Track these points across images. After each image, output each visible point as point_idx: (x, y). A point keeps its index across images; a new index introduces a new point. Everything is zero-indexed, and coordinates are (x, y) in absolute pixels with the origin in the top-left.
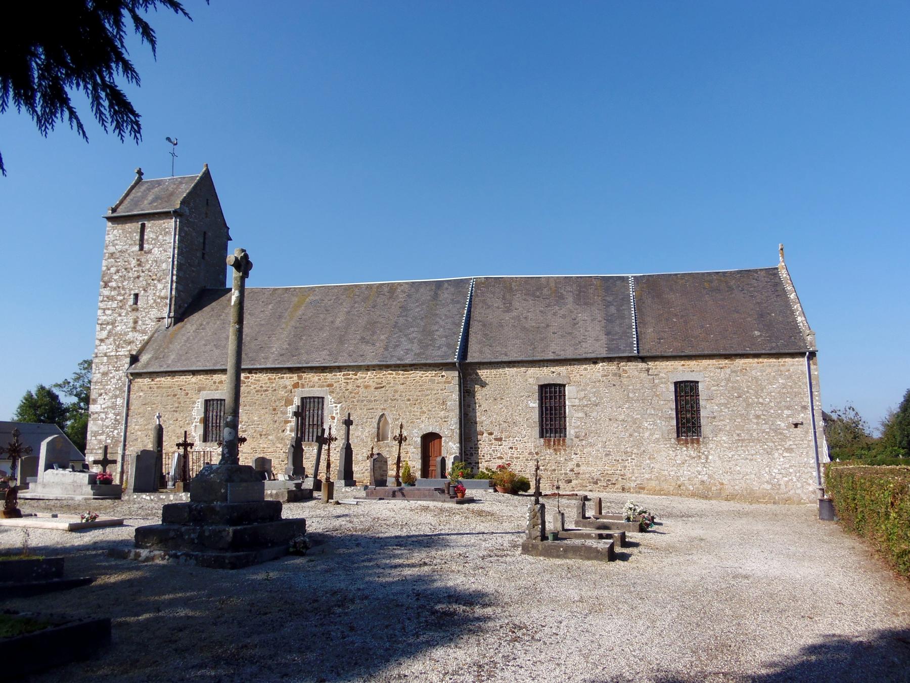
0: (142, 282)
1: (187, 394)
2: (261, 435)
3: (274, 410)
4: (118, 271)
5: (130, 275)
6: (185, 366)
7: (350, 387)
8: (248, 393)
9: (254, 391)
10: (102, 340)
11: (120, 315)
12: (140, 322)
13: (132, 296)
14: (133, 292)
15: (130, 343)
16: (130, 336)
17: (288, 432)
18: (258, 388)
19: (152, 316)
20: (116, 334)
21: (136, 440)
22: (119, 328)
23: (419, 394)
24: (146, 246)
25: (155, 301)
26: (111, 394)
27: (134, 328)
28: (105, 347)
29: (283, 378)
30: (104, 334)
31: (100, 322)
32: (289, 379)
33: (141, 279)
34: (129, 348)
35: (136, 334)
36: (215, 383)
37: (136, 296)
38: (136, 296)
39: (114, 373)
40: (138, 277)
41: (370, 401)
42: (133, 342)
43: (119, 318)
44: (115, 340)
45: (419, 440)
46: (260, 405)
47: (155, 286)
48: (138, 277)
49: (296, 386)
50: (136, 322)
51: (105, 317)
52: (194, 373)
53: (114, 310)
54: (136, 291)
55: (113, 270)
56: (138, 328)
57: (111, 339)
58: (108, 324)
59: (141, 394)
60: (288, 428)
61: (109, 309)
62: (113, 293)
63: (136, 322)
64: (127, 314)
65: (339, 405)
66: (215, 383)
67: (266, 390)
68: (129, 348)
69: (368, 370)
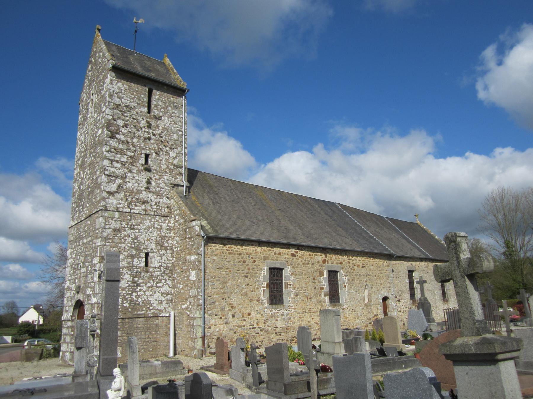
0: (153, 145)
1: (255, 261)
2: (307, 298)
3: (314, 279)
4: (126, 126)
5: (140, 133)
6: (315, 243)
7: (351, 265)
8: (298, 264)
9: (301, 263)
10: (110, 193)
11: (130, 171)
12: (154, 184)
13: (143, 156)
14: (144, 152)
15: (144, 202)
16: (144, 195)
17: (323, 296)
18: (304, 261)
19: (167, 181)
20: (127, 190)
21: (214, 303)
22: (129, 185)
23: (379, 272)
24: (155, 112)
25: (168, 167)
26: (126, 253)
27: (148, 188)
28: (115, 202)
29: (317, 255)
30: (113, 187)
31: (107, 173)
32: (320, 257)
33: (152, 141)
34: (143, 207)
35: (150, 195)
36: (275, 254)
37: (147, 156)
38: (147, 156)
39: (128, 231)
40: (149, 139)
41: (360, 275)
42: (148, 202)
43: (129, 175)
44: (125, 196)
45: (381, 301)
46: (305, 274)
47: (168, 154)
48: (149, 139)
49: (324, 261)
50: (149, 182)
51: (113, 169)
52: (261, 243)
53: (123, 164)
54: (148, 152)
55: (120, 123)
56: (152, 189)
57: (122, 194)
58: (117, 177)
59: (215, 258)
60: (323, 293)
61: (117, 162)
62: (121, 146)
63: (149, 182)
64: (139, 172)
65: (347, 277)
66: (275, 254)
67: (308, 264)
68: (143, 207)
69: (422, 261)
